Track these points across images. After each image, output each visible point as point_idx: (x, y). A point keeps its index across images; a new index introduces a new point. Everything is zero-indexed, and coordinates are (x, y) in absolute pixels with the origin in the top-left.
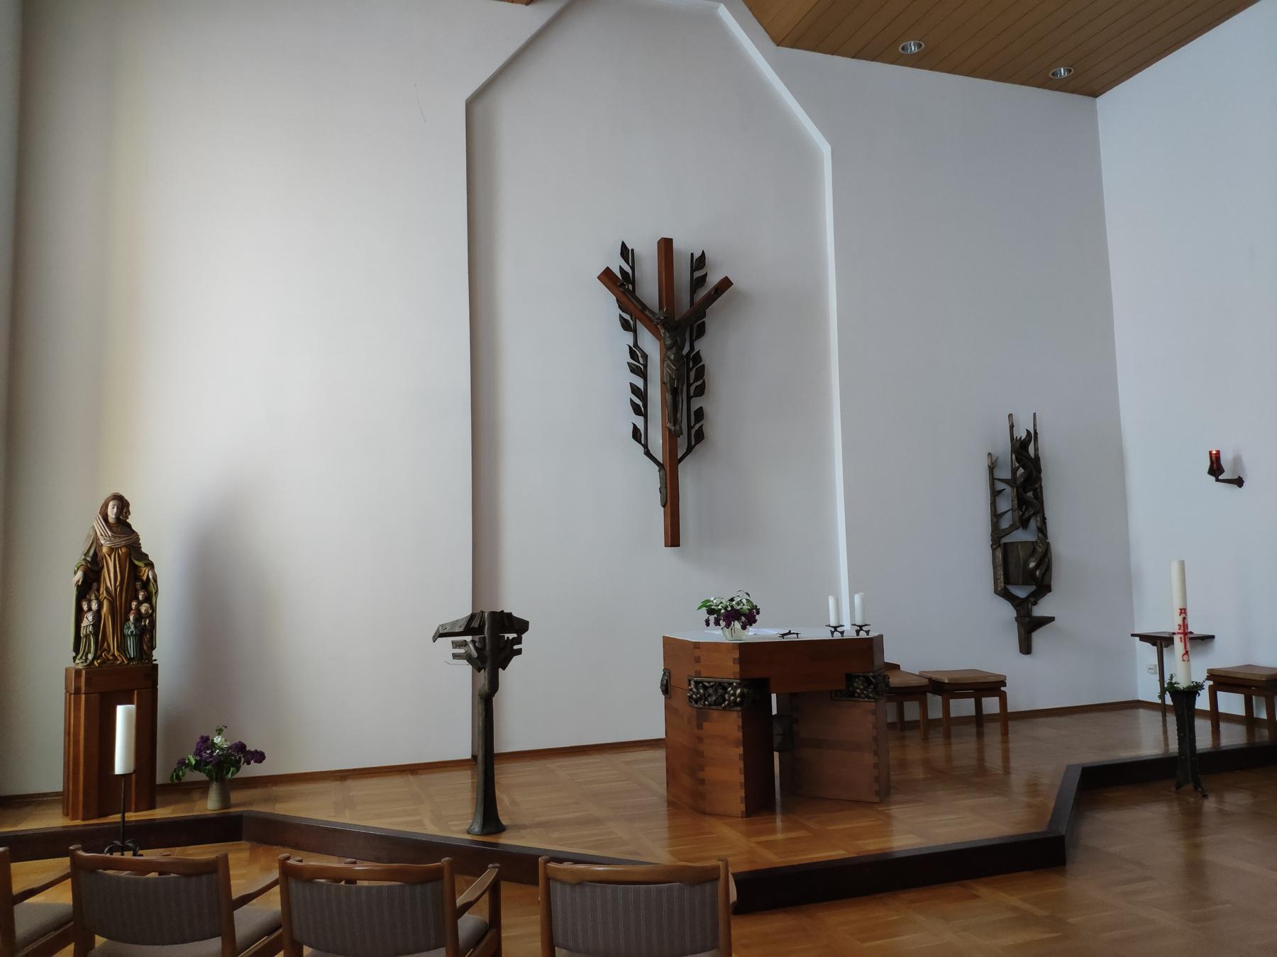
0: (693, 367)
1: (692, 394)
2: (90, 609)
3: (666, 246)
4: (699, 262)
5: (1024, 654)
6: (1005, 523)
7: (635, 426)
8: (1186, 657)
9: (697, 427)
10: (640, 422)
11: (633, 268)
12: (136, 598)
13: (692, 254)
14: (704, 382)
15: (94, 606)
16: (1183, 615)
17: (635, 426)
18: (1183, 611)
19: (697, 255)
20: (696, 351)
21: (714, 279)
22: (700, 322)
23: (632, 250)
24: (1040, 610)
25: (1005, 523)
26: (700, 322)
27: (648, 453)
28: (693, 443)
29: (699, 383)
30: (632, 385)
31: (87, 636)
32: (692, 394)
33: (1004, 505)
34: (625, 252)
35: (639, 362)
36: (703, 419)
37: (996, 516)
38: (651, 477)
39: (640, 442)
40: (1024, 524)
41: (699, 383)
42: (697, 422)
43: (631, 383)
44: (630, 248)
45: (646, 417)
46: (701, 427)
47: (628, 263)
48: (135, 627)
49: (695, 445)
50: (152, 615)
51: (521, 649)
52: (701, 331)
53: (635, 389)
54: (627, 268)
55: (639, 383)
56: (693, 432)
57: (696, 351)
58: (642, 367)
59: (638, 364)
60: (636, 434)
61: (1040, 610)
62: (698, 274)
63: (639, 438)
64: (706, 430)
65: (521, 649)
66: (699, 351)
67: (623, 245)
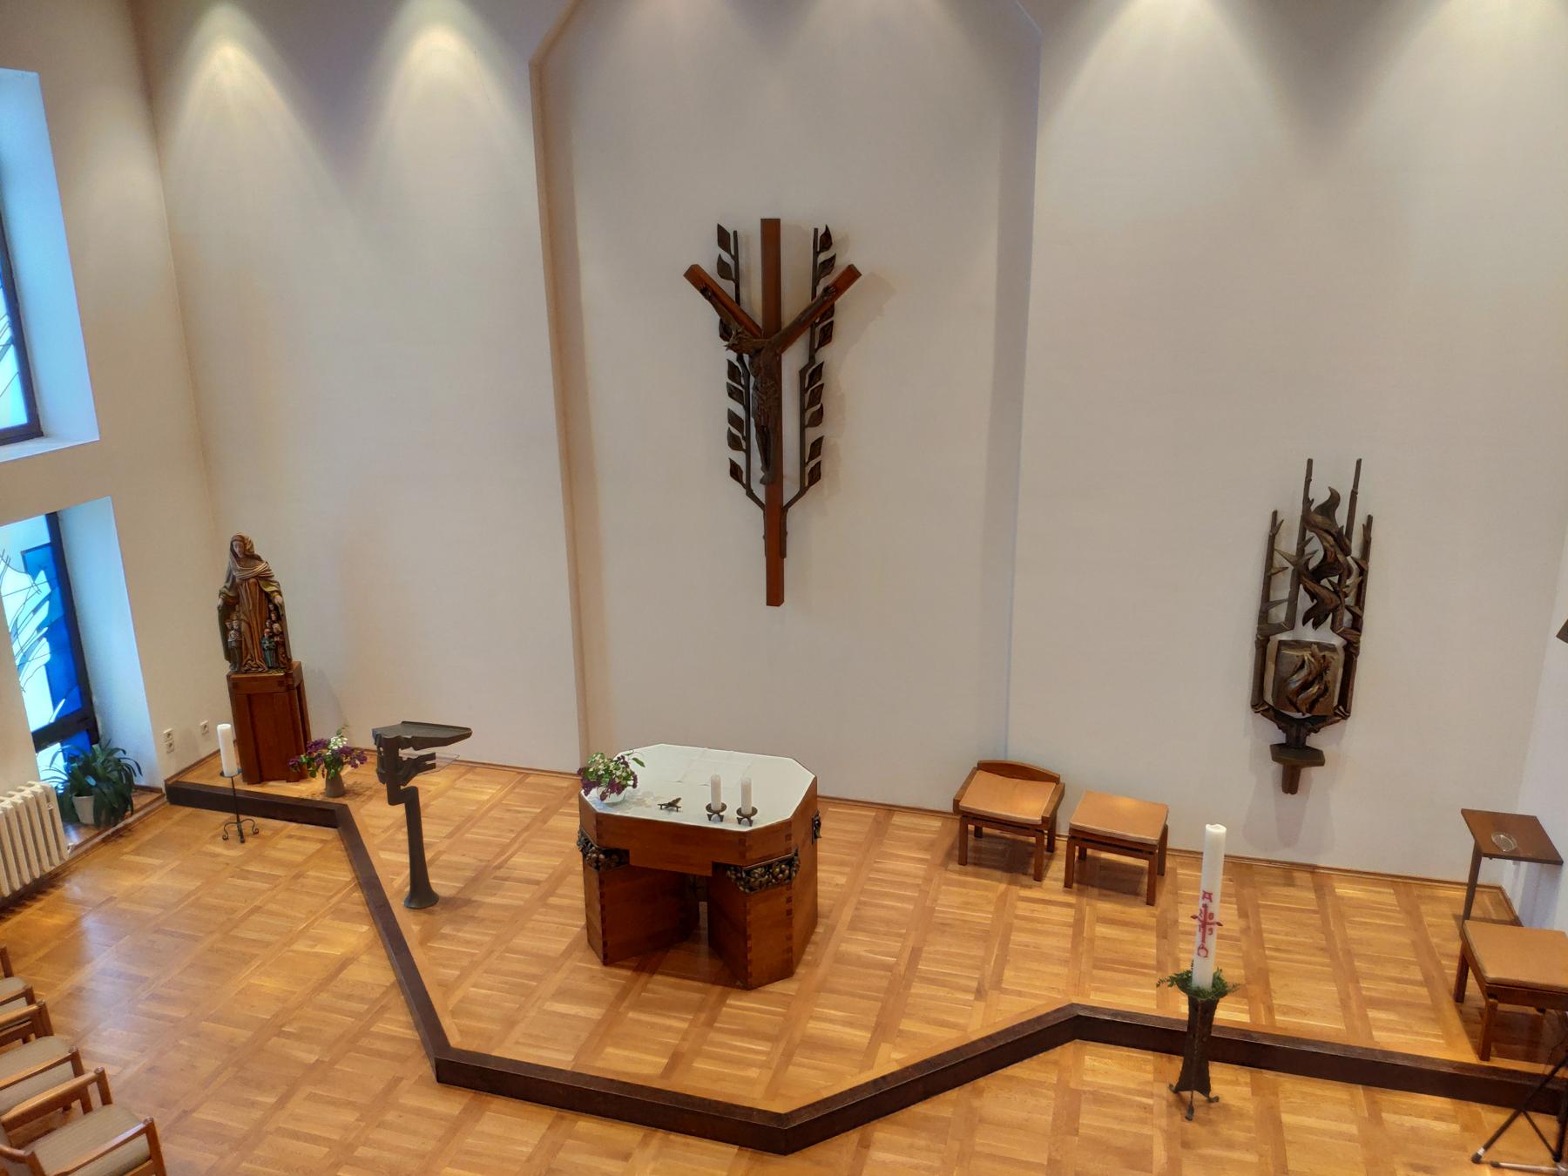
0: (808, 388)
1: (807, 423)
2: (232, 629)
3: (771, 229)
4: (824, 241)
5: (1287, 793)
6: (1279, 614)
8: (1203, 952)
9: (813, 463)
10: (739, 458)
11: (736, 258)
12: (270, 618)
13: (816, 231)
14: (822, 407)
15: (235, 624)
16: (1207, 901)
18: (1207, 896)
19: (821, 232)
20: (818, 362)
21: (841, 264)
22: (829, 321)
23: (735, 233)
24: (1314, 741)
25: (1279, 614)
26: (829, 321)
27: (750, 494)
28: (807, 484)
32: (807, 423)
33: (1282, 590)
34: (724, 238)
36: (819, 454)
37: (1267, 602)
38: (753, 520)
40: (1315, 617)
41: (819, 406)
42: (811, 458)
43: (729, 410)
44: (730, 229)
46: (819, 463)
47: (728, 250)
50: (282, 633)
51: (434, 764)
52: (826, 336)
53: (733, 419)
54: (726, 258)
55: (739, 410)
56: (808, 469)
57: (818, 362)
58: (744, 391)
59: (735, 385)
60: (735, 472)
61: (1314, 741)
62: (822, 257)
64: (825, 469)
65: (434, 764)
66: (822, 364)
67: (720, 230)
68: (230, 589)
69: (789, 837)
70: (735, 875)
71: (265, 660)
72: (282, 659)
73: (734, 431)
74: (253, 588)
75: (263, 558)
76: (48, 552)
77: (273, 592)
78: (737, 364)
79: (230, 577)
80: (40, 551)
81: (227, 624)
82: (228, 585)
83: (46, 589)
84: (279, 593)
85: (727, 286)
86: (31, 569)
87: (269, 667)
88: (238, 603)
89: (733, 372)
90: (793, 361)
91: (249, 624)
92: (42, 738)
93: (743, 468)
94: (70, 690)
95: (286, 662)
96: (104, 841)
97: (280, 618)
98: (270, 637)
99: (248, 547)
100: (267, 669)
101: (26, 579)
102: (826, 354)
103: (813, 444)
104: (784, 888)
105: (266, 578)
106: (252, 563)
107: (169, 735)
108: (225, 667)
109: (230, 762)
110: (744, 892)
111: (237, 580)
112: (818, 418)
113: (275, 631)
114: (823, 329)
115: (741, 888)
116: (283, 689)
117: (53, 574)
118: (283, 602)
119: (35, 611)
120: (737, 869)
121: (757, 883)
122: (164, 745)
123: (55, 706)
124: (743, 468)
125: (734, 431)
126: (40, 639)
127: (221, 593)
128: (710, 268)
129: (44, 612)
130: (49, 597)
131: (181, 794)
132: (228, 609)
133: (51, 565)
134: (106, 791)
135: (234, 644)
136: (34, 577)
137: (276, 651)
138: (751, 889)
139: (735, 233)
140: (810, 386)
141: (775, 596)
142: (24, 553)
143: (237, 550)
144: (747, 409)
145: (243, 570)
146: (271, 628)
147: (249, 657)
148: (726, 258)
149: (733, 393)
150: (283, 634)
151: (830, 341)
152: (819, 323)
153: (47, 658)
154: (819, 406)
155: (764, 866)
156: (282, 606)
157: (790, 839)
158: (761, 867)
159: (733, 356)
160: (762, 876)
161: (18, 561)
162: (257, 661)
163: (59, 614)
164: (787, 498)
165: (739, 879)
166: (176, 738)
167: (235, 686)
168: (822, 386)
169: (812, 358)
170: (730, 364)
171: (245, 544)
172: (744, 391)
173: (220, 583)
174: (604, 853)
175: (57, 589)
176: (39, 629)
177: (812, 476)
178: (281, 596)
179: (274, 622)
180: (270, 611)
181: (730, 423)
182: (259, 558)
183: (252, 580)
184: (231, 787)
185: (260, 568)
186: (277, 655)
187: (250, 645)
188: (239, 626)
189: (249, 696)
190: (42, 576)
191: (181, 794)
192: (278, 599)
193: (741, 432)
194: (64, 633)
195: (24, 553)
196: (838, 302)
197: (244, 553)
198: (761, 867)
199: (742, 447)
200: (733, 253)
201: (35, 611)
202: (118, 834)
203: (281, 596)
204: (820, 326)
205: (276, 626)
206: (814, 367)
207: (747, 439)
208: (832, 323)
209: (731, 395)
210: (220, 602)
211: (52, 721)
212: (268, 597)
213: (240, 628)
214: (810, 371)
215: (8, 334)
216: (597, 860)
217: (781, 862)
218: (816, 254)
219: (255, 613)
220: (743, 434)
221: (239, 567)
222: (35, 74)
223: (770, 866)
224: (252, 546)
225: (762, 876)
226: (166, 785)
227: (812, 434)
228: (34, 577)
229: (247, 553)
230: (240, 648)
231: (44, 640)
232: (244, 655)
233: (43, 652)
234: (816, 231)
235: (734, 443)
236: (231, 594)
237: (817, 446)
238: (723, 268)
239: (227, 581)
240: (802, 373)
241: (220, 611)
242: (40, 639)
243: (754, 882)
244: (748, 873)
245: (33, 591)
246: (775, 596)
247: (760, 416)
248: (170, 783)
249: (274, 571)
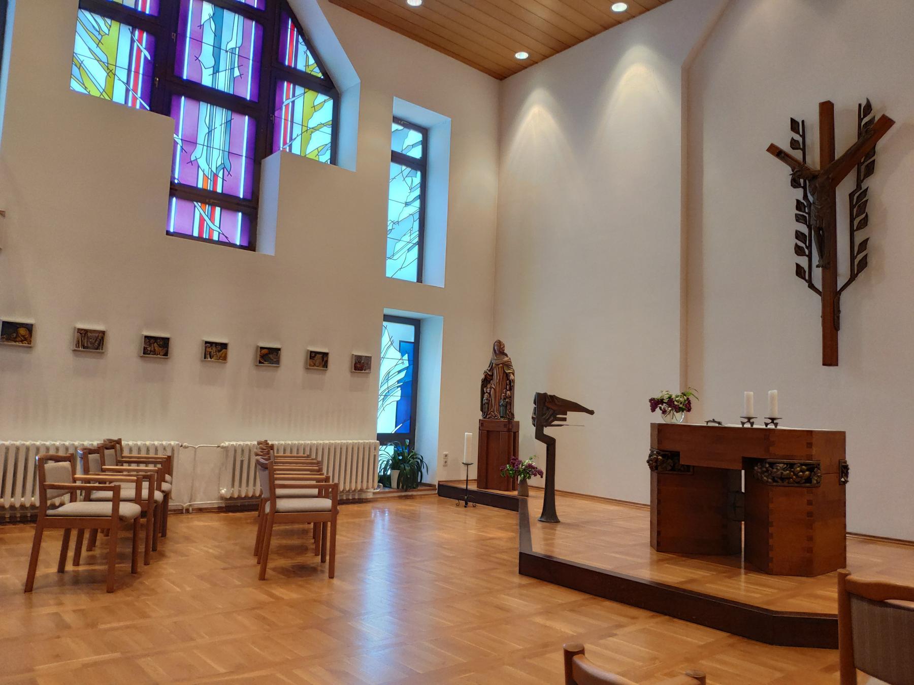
1: (855, 228)
2: (487, 392)
3: (827, 109)
4: (867, 108)
7: (798, 265)
10: (803, 262)
11: (803, 136)
12: (506, 389)
14: (867, 216)
17: (798, 265)
19: (864, 103)
20: (864, 187)
23: (803, 122)
27: (811, 286)
29: (864, 216)
30: (797, 232)
31: (485, 404)
32: (855, 228)
34: (794, 123)
35: (805, 212)
38: (815, 303)
39: (804, 278)
41: (864, 216)
42: (859, 253)
45: (810, 257)
46: (866, 256)
47: (798, 133)
48: (504, 402)
49: (857, 274)
51: (566, 418)
52: (870, 170)
53: (799, 235)
54: (797, 137)
55: (804, 229)
56: (856, 263)
57: (864, 187)
58: (807, 215)
60: (800, 271)
63: (803, 274)
68: (490, 371)
69: (810, 445)
70: (761, 468)
71: (500, 413)
72: (508, 412)
73: (801, 244)
74: (500, 369)
75: (508, 355)
76: (410, 347)
77: (510, 373)
78: (803, 201)
79: (491, 364)
80: (408, 344)
81: (485, 389)
82: (489, 369)
83: (406, 364)
84: (514, 375)
85: (797, 155)
86: (402, 351)
87: (501, 417)
88: (492, 379)
89: (799, 205)
90: (843, 192)
91: (495, 390)
92: (384, 439)
93: (806, 269)
94: (405, 421)
95: (510, 414)
96: (400, 497)
97: (511, 389)
98: (505, 399)
99: (502, 347)
100: (500, 418)
101: (398, 355)
102: (873, 183)
103: (860, 244)
104: (805, 490)
105: (508, 365)
106: (502, 357)
107: (446, 456)
108: (479, 415)
109: (473, 474)
110: (767, 481)
111: (494, 365)
112: (864, 223)
113: (507, 395)
114: (867, 166)
115: (765, 478)
116: (506, 429)
117: (412, 359)
118: (514, 379)
119: (399, 372)
120: (761, 461)
121: (779, 473)
122: (443, 463)
123: (396, 427)
124: (806, 269)
125: (801, 244)
126: (398, 387)
127: (485, 372)
128: (785, 146)
129: (402, 375)
130: (407, 368)
131: (447, 491)
132: (486, 381)
133: (411, 354)
134: (406, 468)
135: (486, 401)
136: (402, 356)
137: (506, 406)
138: (774, 481)
139: (803, 122)
140: (857, 203)
141: (830, 357)
142: (400, 342)
143: (496, 348)
144: (809, 227)
145: (497, 359)
146: (506, 394)
147: (492, 410)
148: (797, 137)
149: (798, 218)
150: (511, 397)
151: (872, 173)
152: (864, 162)
153: (399, 398)
154: (864, 215)
155: (787, 464)
156: (513, 381)
157: (811, 447)
158: (784, 463)
159: (799, 194)
160: (784, 469)
161: (397, 344)
162: (496, 413)
163: (409, 379)
164: (840, 284)
165: (763, 472)
166: (449, 460)
167: (482, 423)
168: (867, 201)
169: (859, 186)
170: (798, 201)
171: (501, 345)
172: (807, 215)
173: (486, 367)
174: (663, 456)
175: (412, 366)
176: (398, 382)
177: (859, 266)
178: (514, 375)
179: (508, 390)
180: (507, 385)
181: (797, 238)
182: (506, 355)
183: (501, 365)
184: (466, 479)
185: (506, 359)
186: (506, 411)
187: (493, 402)
188: (490, 391)
189: (488, 431)
190: (406, 357)
191: (447, 491)
192: (512, 377)
193: (805, 244)
194: (409, 389)
195: (400, 342)
196: (881, 144)
197: (499, 350)
198: (784, 463)
199: (805, 252)
200: (801, 133)
201: (399, 372)
202: (407, 497)
203: (514, 375)
204: (866, 163)
205: (508, 392)
206: (861, 191)
207: (810, 247)
208: (874, 161)
209: (797, 221)
210: (483, 376)
211: (393, 432)
212: (507, 376)
213: (490, 392)
214: (856, 195)
215: (417, 240)
216: (657, 460)
217: (802, 465)
218: (860, 120)
219: (499, 385)
220: (806, 245)
221: (495, 358)
222: (450, 119)
223: (791, 466)
224: (504, 346)
225: (784, 469)
226: (439, 485)
227: (859, 237)
228: (402, 356)
229: (501, 350)
230: (488, 404)
231: (400, 388)
232: (490, 408)
233: (397, 395)
234: (860, 105)
235: (799, 251)
236: (489, 373)
237: (864, 245)
238: (794, 144)
239: (489, 367)
240: (851, 195)
241: (482, 382)
242: (398, 387)
243: (776, 472)
244: (772, 465)
245: (400, 362)
246: (830, 357)
247: (816, 221)
248: (441, 483)
249: (513, 364)
